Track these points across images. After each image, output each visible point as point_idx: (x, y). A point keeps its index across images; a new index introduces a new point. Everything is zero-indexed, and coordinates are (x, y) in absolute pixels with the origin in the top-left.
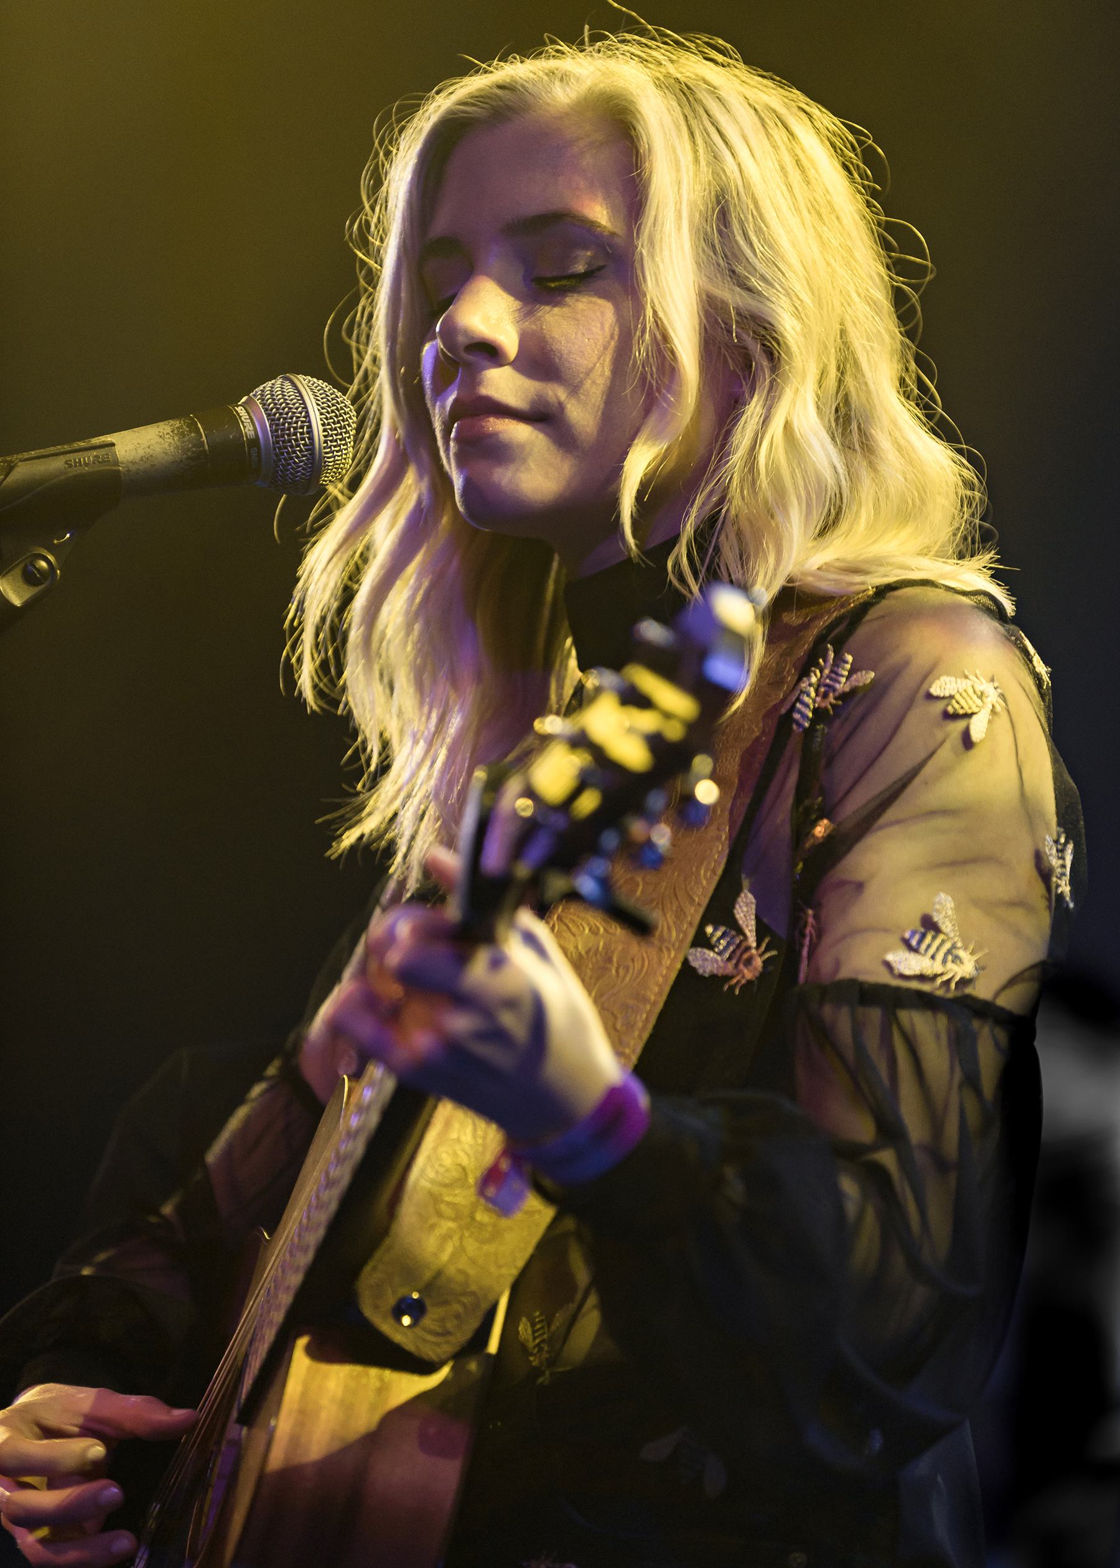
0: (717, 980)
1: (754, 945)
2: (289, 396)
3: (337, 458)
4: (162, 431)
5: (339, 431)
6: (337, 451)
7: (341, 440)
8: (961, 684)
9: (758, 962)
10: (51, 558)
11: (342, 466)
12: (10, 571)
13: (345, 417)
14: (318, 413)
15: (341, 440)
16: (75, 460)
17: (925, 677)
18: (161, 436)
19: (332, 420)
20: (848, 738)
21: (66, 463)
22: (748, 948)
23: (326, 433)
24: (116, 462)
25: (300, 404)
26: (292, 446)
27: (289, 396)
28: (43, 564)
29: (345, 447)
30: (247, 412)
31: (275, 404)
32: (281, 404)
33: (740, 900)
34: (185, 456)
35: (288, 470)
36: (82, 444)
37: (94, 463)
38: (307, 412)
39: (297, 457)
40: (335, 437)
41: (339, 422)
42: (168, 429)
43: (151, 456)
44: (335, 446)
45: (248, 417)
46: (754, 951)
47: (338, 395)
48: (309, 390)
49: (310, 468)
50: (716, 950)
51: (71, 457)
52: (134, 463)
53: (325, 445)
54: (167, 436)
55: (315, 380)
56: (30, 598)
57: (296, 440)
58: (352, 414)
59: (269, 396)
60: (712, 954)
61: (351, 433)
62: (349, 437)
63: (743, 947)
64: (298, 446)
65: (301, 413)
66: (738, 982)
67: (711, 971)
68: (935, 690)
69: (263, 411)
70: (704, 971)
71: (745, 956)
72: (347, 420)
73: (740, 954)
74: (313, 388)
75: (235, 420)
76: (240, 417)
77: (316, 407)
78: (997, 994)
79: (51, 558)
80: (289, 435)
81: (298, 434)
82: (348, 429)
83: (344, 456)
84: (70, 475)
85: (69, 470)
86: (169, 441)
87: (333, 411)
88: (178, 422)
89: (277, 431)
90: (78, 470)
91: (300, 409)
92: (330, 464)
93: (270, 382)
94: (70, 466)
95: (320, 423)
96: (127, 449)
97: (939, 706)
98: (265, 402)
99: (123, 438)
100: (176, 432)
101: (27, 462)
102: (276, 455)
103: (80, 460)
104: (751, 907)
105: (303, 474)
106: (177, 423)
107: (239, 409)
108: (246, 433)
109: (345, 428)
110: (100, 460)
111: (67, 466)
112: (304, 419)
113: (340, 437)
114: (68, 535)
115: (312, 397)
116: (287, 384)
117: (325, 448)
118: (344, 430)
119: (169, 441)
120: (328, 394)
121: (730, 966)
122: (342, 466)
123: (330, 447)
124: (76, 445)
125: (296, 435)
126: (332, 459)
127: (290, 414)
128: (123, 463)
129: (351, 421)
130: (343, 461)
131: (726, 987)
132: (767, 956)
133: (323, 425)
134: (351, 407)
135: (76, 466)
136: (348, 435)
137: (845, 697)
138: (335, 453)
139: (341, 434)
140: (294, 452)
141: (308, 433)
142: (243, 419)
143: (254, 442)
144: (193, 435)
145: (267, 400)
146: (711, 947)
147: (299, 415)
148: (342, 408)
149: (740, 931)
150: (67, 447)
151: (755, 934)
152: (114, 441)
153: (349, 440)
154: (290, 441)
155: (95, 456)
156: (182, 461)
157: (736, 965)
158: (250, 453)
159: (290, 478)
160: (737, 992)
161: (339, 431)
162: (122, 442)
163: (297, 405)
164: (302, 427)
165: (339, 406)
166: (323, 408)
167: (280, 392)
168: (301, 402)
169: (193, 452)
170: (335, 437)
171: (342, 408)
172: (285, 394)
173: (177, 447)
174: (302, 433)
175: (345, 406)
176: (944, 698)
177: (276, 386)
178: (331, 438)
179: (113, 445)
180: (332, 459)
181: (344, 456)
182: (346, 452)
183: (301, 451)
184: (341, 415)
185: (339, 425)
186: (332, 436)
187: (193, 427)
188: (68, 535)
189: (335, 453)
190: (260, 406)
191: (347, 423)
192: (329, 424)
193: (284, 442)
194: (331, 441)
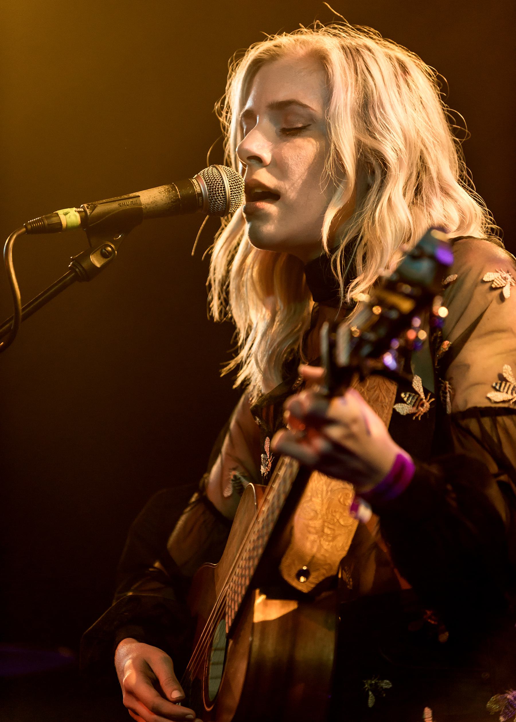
0: (409, 416)
1: (424, 398)
2: (215, 174)
3: (236, 201)
5: (237, 189)
6: (236, 198)
7: (238, 193)
8: (496, 275)
9: (427, 405)
10: (113, 246)
11: (238, 204)
12: (93, 253)
13: (240, 183)
14: (228, 181)
15: (238, 193)
16: (123, 203)
17: (480, 274)
18: (160, 193)
19: (234, 185)
21: (119, 204)
22: (422, 399)
23: (232, 190)
24: (141, 204)
25: (220, 178)
26: (217, 196)
27: (215, 174)
28: (109, 249)
29: (240, 196)
30: (197, 181)
31: (209, 178)
32: (212, 178)
33: (414, 380)
34: (170, 201)
35: (215, 206)
36: (126, 196)
37: (131, 205)
38: (223, 181)
39: (219, 201)
40: (235, 192)
41: (237, 185)
42: (163, 190)
43: (156, 201)
44: (235, 196)
45: (197, 184)
46: (424, 400)
47: (236, 173)
48: (224, 172)
49: (225, 205)
50: (407, 403)
51: (121, 202)
52: (148, 204)
53: (231, 195)
54: (163, 192)
55: (226, 167)
56: (104, 263)
57: (218, 193)
58: (242, 182)
59: (206, 174)
60: (405, 405)
61: (242, 190)
62: (241, 192)
63: (419, 399)
64: (219, 196)
65: (220, 181)
66: (419, 415)
67: (406, 412)
68: (485, 279)
69: (204, 181)
70: (404, 413)
71: (421, 403)
72: (240, 184)
73: (419, 403)
74: (226, 170)
75: (192, 185)
76: (194, 184)
77: (227, 179)
79: (113, 246)
80: (215, 191)
81: (219, 191)
82: (241, 188)
83: (239, 200)
85: (120, 207)
86: (163, 194)
87: (234, 181)
88: (167, 186)
89: (210, 189)
90: (124, 208)
91: (220, 180)
92: (233, 204)
93: (207, 168)
94: (121, 206)
95: (229, 186)
97: (488, 285)
98: (205, 177)
99: (143, 193)
100: (166, 190)
101: (102, 205)
102: (210, 200)
103: (125, 203)
104: (419, 382)
105: (221, 208)
106: (167, 187)
107: (193, 180)
108: (197, 191)
109: (239, 187)
110: (134, 203)
112: (222, 184)
113: (238, 192)
114: (120, 236)
115: (225, 175)
116: (214, 169)
117: (231, 196)
118: (239, 189)
119: (163, 194)
120: (232, 173)
121: (415, 408)
122: (238, 204)
123: (233, 196)
124: (123, 197)
125: (218, 191)
126: (234, 201)
127: (216, 182)
128: (143, 204)
129: (242, 185)
130: (239, 202)
131: (414, 418)
132: (431, 401)
133: (230, 186)
134: (242, 178)
135: (123, 206)
136: (241, 191)
138: (236, 199)
139: (238, 190)
140: (218, 199)
141: (223, 190)
142: (195, 184)
143: (201, 194)
144: (174, 192)
145: (206, 176)
146: (404, 402)
147: (220, 182)
148: (238, 179)
149: (416, 393)
150: (119, 198)
151: (423, 393)
152: (140, 195)
153: (242, 193)
154: (216, 194)
155: (131, 202)
156: (169, 203)
157: (417, 408)
158: (198, 199)
159: (216, 210)
160: (420, 419)
161: (237, 189)
162: (143, 195)
163: (219, 178)
164: (221, 188)
165: (237, 178)
166: (230, 179)
167: (211, 173)
168: (220, 177)
169: (174, 199)
170: (235, 192)
171: (238, 179)
172: (213, 173)
174: (221, 190)
175: (240, 178)
176: (489, 282)
177: (210, 170)
178: (234, 192)
179: (139, 196)
180: (234, 201)
181: (239, 200)
182: (240, 198)
183: (221, 198)
184: (238, 182)
185: (237, 186)
186: (234, 191)
187: (173, 188)
188: (120, 236)
189: (236, 199)
190: (203, 179)
191: (240, 185)
192: (233, 186)
193: (213, 194)
194: (234, 194)
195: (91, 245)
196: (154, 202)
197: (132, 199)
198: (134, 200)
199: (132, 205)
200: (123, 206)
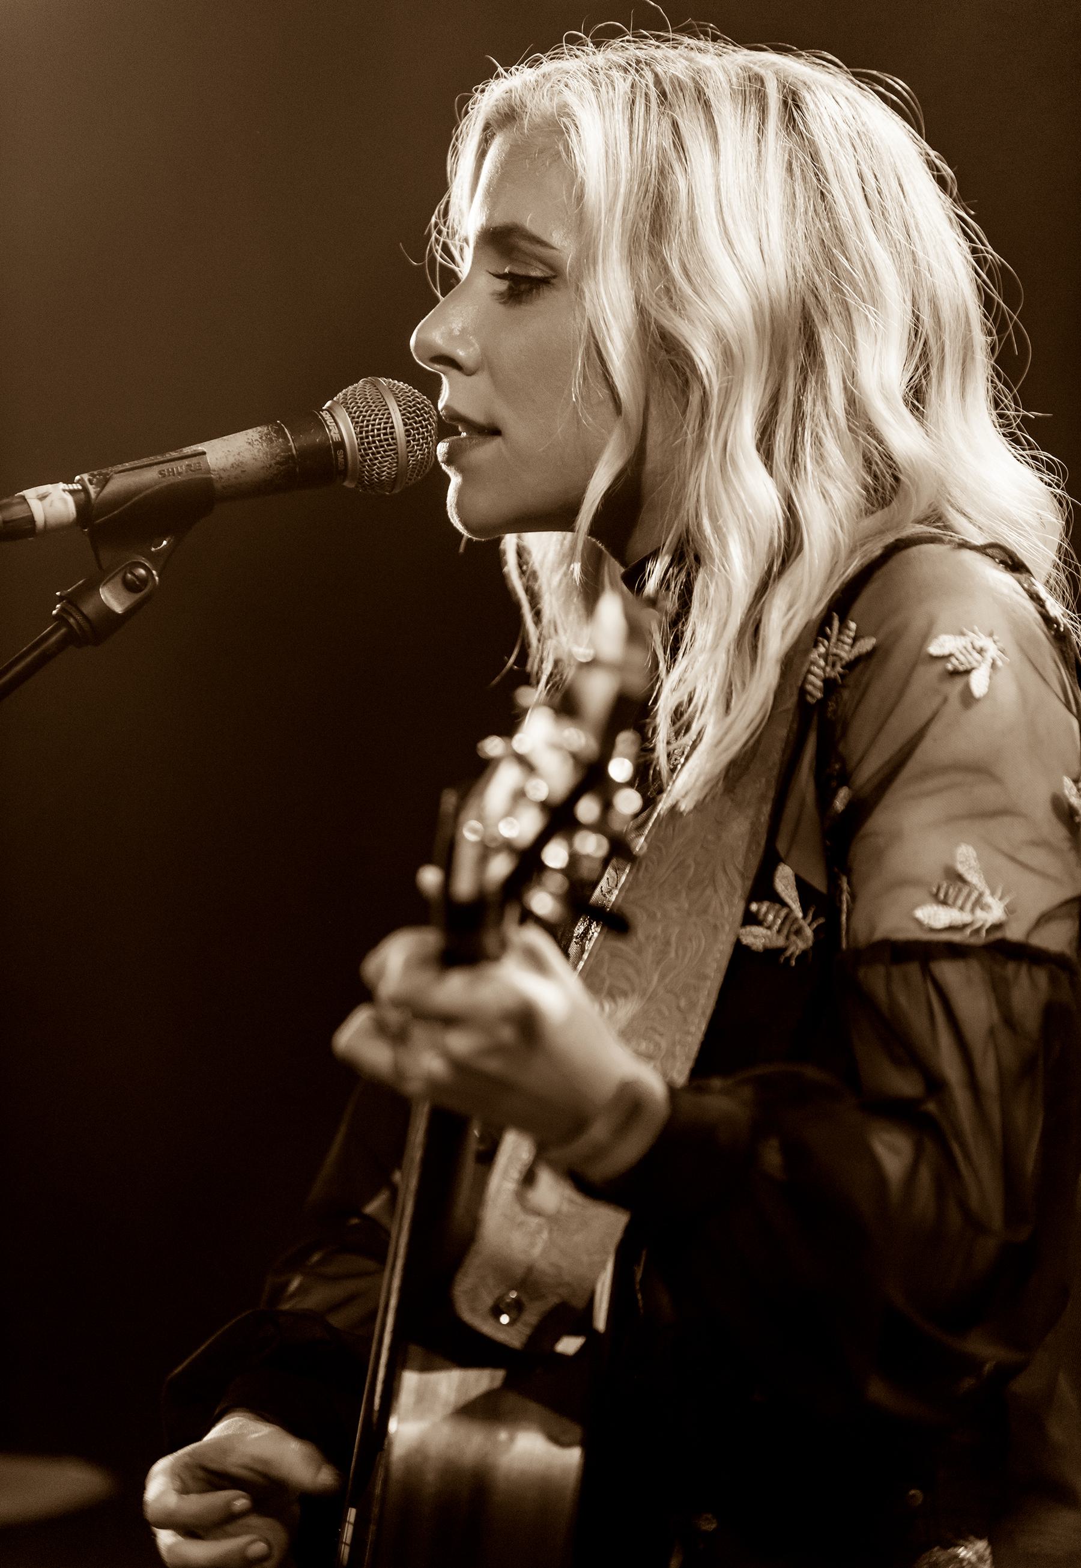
4: (250, 437)
16: (168, 470)
18: (250, 443)
20: (859, 702)
24: (208, 471)
36: (174, 454)
37: (187, 472)
42: (257, 436)
43: (242, 463)
51: (165, 467)
52: (224, 470)
78: (1029, 934)
84: (165, 484)
85: (163, 479)
86: (258, 447)
88: (266, 428)
90: (172, 480)
94: (164, 476)
96: (218, 457)
98: (350, 410)
99: (213, 446)
100: (264, 438)
103: (173, 469)
110: (192, 468)
111: (160, 476)
119: (258, 447)
124: (168, 456)
135: (170, 475)
137: (850, 666)
144: (281, 440)
150: (160, 458)
152: (205, 450)
155: (188, 465)
173: (266, 453)
179: (204, 453)
195: (100, 567)
196: (238, 466)
197: (189, 459)
198: (194, 460)
199: (190, 472)
200: (170, 475)
